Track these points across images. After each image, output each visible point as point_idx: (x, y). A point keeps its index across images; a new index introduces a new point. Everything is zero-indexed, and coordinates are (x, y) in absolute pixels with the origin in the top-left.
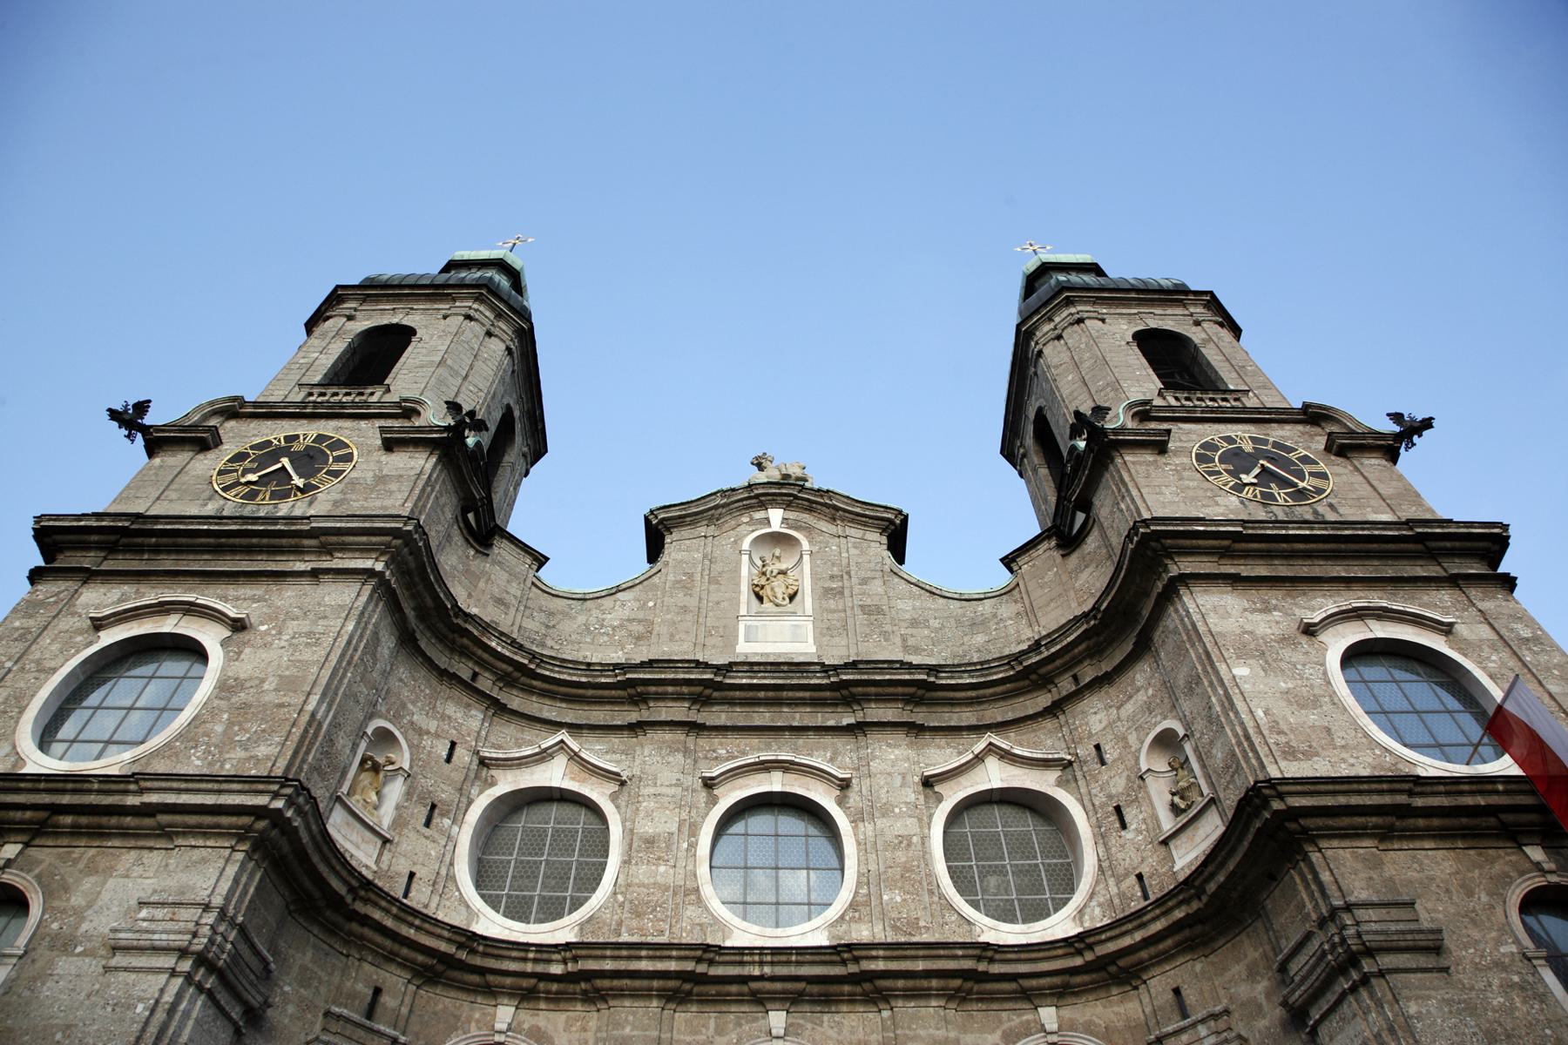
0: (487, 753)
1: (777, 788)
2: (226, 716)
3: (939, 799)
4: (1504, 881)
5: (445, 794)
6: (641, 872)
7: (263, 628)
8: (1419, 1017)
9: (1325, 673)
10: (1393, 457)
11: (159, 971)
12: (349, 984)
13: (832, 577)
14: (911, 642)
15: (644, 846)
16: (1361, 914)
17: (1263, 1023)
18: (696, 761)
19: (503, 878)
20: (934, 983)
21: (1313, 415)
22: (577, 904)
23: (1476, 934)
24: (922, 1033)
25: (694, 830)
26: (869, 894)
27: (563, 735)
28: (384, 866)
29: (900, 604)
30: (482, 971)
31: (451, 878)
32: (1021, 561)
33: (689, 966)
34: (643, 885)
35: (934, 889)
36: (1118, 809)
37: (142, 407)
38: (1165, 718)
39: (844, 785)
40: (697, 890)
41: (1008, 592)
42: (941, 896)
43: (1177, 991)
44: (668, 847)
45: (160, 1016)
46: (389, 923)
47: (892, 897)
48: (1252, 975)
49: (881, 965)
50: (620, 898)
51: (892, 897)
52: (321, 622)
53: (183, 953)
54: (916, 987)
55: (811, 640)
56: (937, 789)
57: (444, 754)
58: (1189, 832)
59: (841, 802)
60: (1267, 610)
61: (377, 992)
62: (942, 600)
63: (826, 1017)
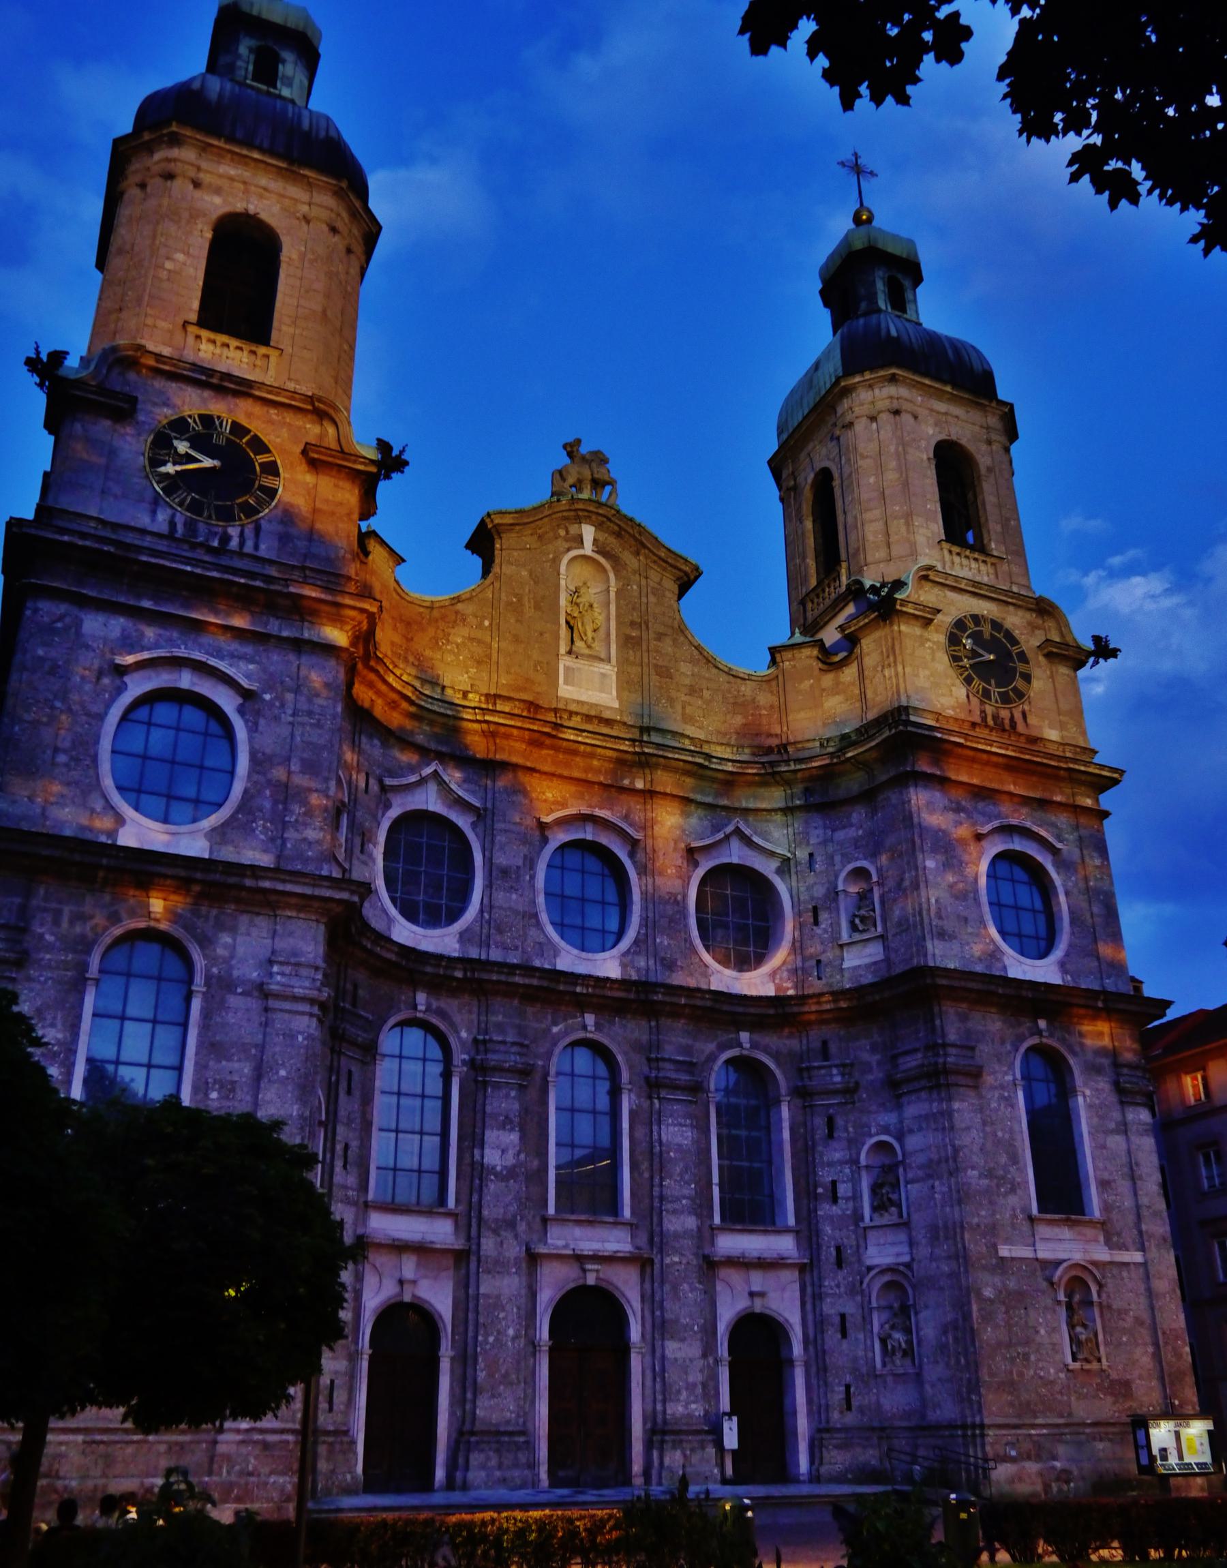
0: (388, 781)
1: (589, 837)
2: (268, 792)
3: (696, 864)
4: (1021, 1039)
6: (500, 897)
7: (267, 697)
8: (958, 1111)
10: (1080, 664)
11: (303, 1013)
13: (632, 624)
17: (870, 1077)
21: (1043, 609)
24: (674, 1039)
25: (531, 863)
26: (646, 935)
29: (685, 668)
32: (788, 655)
33: (545, 984)
34: (501, 908)
35: (688, 940)
38: (865, 859)
41: (768, 680)
42: (691, 944)
44: (518, 878)
46: (369, 946)
48: (874, 1049)
50: (486, 916)
53: (312, 1001)
54: (675, 1012)
55: (614, 693)
58: (859, 946)
59: (632, 855)
61: (356, 987)
62: (714, 671)
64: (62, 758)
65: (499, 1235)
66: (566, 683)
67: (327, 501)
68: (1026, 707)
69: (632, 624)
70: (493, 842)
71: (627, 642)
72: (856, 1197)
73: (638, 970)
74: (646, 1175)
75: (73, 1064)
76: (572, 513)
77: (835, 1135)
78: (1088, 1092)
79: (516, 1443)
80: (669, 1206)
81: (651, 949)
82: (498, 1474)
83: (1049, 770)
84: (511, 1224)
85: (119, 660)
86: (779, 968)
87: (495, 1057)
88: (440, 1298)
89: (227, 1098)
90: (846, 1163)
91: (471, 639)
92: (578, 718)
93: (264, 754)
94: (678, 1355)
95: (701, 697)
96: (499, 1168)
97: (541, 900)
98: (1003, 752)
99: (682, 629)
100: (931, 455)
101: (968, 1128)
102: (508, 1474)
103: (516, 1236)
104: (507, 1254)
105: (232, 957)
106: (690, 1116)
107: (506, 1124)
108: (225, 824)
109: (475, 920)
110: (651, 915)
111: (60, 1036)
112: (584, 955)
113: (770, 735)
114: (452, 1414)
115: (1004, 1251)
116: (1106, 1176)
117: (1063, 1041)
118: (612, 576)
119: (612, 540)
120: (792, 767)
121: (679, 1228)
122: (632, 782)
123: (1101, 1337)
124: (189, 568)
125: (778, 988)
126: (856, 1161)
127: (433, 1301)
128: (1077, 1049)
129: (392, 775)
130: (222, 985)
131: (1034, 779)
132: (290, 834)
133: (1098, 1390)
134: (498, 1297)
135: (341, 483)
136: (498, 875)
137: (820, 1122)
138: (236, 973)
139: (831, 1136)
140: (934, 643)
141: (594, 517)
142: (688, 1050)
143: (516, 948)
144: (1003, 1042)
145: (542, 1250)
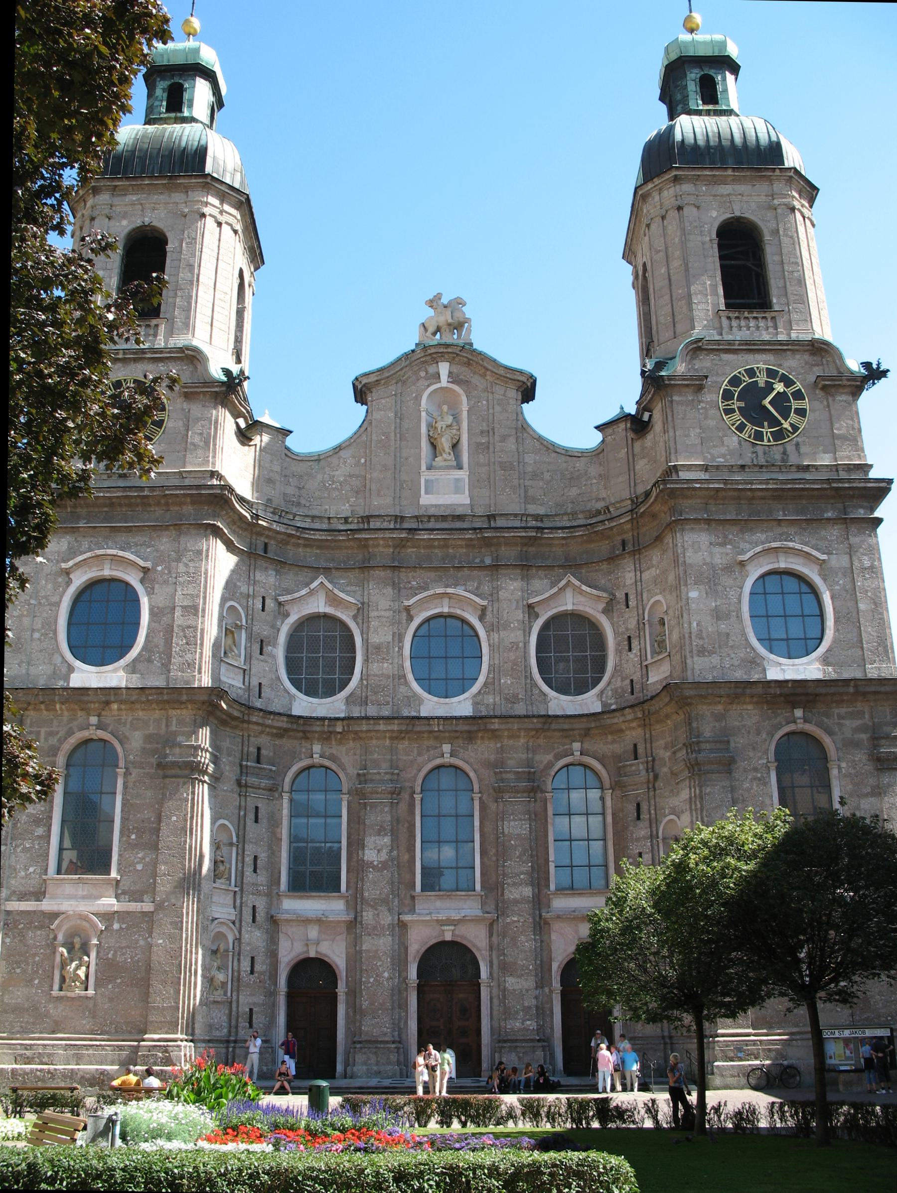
0: (281, 599)
1: (446, 610)
3: (537, 616)
4: (778, 727)
5: (266, 632)
6: (375, 667)
7: (159, 568)
9: (740, 595)
12: (246, 749)
13: (482, 432)
18: (399, 591)
19: (301, 667)
22: (344, 684)
23: (751, 754)
25: (401, 638)
30: (304, 732)
31: (278, 678)
34: (375, 675)
36: (629, 637)
38: (661, 593)
39: (484, 609)
40: (404, 676)
41: (598, 453)
42: (532, 679)
43: (635, 746)
44: (388, 652)
47: (506, 681)
48: (666, 748)
49: (496, 726)
50: (365, 682)
51: (506, 681)
52: (191, 564)
55: (467, 492)
59: (481, 618)
60: (723, 544)
61: (259, 749)
62: (554, 455)
64: (36, 635)
65: (376, 909)
66: (427, 493)
70: (368, 627)
71: (477, 448)
74: (494, 858)
75: (51, 825)
76: (428, 358)
77: (641, 817)
78: (844, 765)
79: (389, 1048)
80: (509, 881)
81: (497, 688)
82: (375, 1068)
83: (816, 493)
84: (385, 901)
85: (64, 565)
86: (605, 689)
88: (336, 953)
90: (648, 838)
91: (350, 476)
93: (158, 608)
94: (516, 987)
95: (542, 479)
96: (375, 863)
97: (407, 664)
99: (523, 428)
100: (714, 236)
102: (382, 1068)
103: (389, 910)
104: (382, 922)
106: (529, 812)
107: (380, 832)
110: (497, 662)
111: (43, 809)
112: (442, 700)
113: (598, 500)
114: (348, 1029)
117: (819, 725)
118: (464, 398)
119: (464, 369)
121: (518, 896)
122: (482, 561)
125: (604, 705)
127: (331, 955)
129: (289, 592)
134: (376, 951)
137: (631, 808)
139: (638, 818)
140: (707, 402)
141: (446, 356)
142: (529, 764)
143: (388, 703)
144: (758, 733)
145: (406, 918)
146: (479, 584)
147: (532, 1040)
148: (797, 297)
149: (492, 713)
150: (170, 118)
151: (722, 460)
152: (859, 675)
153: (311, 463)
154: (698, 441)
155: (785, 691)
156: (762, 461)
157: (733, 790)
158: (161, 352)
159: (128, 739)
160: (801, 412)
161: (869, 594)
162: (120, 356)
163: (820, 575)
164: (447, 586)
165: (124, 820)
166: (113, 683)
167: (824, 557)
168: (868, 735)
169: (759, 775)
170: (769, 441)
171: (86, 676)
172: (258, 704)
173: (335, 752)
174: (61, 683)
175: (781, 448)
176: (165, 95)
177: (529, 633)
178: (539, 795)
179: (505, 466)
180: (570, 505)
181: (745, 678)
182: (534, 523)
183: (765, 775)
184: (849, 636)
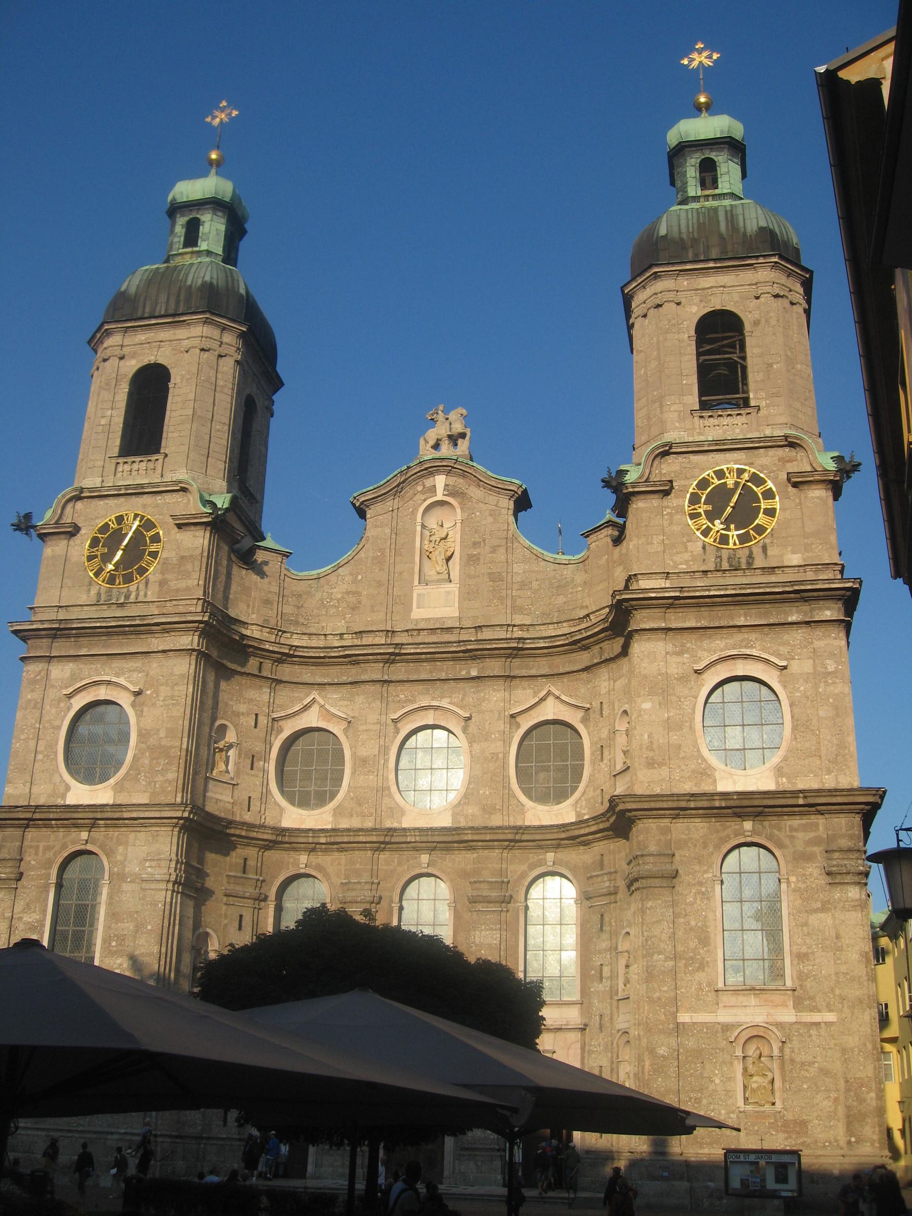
1: (431, 722)
3: (518, 726)
4: (725, 840)
5: (258, 747)
7: (148, 692)
9: (695, 705)
11: (162, 890)
13: (475, 544)
14: (519, 602)
15: (362, 763)
16: (647, 859)
20: (496, 843)
22: (333, 795)
24: (490, 866)
27: (314, 694)
28: (236, 798)
31: (268, 791)
33: (382, 839)
34: (362, 787)
37: (28, 516)
40: (389, 788)
45: (168, 907)
46: (243, 833)
49: (470, 837)
50: (352, 794)
52: (176, 688)
54: (488, 844)
55: (457, 605)
56: (518, 719)
57: (253, 724)
59: (465, 729)
60: (680, 653)
61: (245, 859)
62: (543, 563)
63: (448, 857)
67: (188, 549)
68: (767, 541)
69: (475, 544)
71: (471, 560)
72: (613, 976)
73: (466, 817)
78: (793, 879)
86: (580, 799)
87: (353, 894)
89: (121, 945)
91: (348, 593)
92: (425, 632)
95: (530, 589)
98: (722, 593)
100: (693, 333)
101: (658, 922)
105: (125, 860)
108: (124, 779)
109: (344, 799)
115: (684, 1017)
116: (804, 949)
117: (770, 838)
118: (459, 511)
119: (461, 481)
120: (585, 635)
122: (468, 672)
123: (778, 1084)
124: (98, 625)
125: (578, 814)
126: (616, 948)
128: (787, 841)
130: (119, 878)
131: (767, 606)
132: (160, 778)
133: (770, 1127)
135: (197, 534)
136: (362, 763)
138: (127, 870)
139: (601, 929)
146: (464, 695)
147: (492, 1150)
148: (775, 390)
149: (470, 824)
150: (186, 253)
151: (684, 566)
152: (815, 786)
153: (311, 582)
154: (660, 549)
155: (731, 803)
156: (725, 565)
157: (674, 904)
158: (158, 486)
159: (114, 853)
160: (770, 513)
161: (831, 700)
162: (123, 492)
163: (780, 682)
164: (433, 699)
165: (107, 927)
166: (104, 802)
167: (784, 663)
168: (821, 848)
169: (703, 889)
170: (735, 544)
171: (80, 794)
172: (248, 817)
173: (321, 862)
174: (60, 802)
175: (747, 552)
176: (184, 230)
177: (510, 744)
178: (511, 906)
179: (494, 577)
180: (556, 614)
181: (695, 790)
182: (518, 633)
183: (709, 890)
184: (808, 744)
